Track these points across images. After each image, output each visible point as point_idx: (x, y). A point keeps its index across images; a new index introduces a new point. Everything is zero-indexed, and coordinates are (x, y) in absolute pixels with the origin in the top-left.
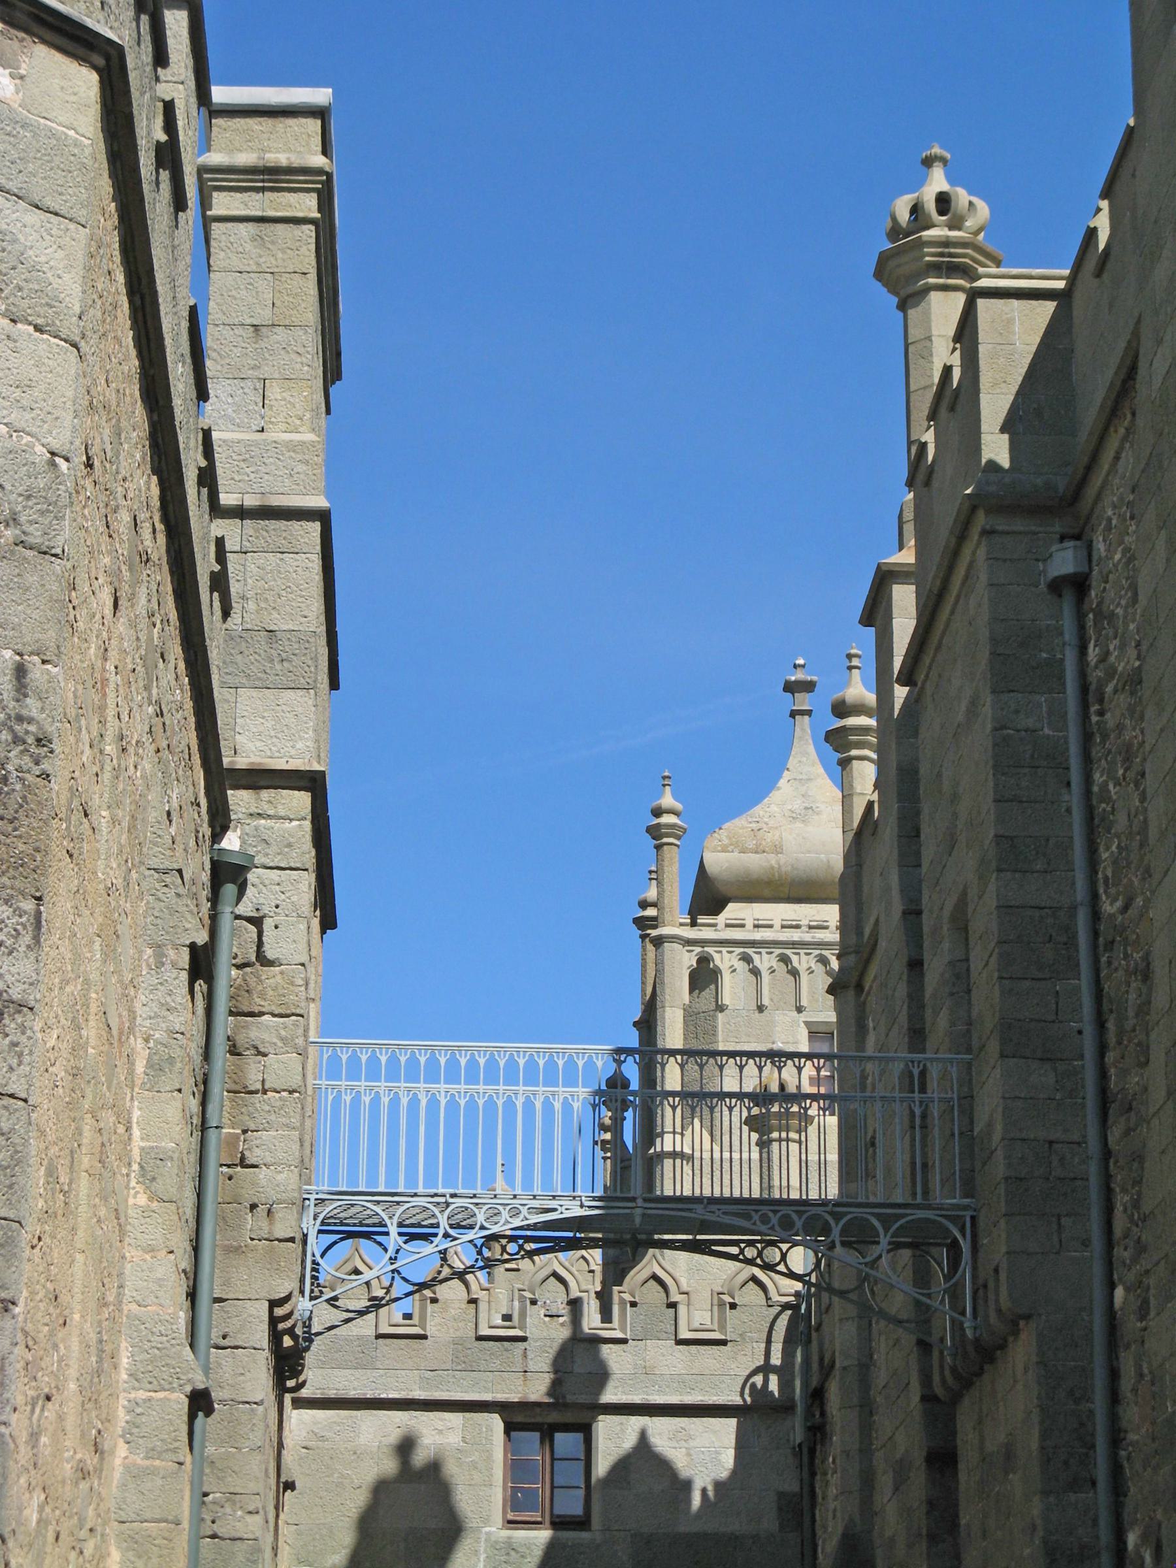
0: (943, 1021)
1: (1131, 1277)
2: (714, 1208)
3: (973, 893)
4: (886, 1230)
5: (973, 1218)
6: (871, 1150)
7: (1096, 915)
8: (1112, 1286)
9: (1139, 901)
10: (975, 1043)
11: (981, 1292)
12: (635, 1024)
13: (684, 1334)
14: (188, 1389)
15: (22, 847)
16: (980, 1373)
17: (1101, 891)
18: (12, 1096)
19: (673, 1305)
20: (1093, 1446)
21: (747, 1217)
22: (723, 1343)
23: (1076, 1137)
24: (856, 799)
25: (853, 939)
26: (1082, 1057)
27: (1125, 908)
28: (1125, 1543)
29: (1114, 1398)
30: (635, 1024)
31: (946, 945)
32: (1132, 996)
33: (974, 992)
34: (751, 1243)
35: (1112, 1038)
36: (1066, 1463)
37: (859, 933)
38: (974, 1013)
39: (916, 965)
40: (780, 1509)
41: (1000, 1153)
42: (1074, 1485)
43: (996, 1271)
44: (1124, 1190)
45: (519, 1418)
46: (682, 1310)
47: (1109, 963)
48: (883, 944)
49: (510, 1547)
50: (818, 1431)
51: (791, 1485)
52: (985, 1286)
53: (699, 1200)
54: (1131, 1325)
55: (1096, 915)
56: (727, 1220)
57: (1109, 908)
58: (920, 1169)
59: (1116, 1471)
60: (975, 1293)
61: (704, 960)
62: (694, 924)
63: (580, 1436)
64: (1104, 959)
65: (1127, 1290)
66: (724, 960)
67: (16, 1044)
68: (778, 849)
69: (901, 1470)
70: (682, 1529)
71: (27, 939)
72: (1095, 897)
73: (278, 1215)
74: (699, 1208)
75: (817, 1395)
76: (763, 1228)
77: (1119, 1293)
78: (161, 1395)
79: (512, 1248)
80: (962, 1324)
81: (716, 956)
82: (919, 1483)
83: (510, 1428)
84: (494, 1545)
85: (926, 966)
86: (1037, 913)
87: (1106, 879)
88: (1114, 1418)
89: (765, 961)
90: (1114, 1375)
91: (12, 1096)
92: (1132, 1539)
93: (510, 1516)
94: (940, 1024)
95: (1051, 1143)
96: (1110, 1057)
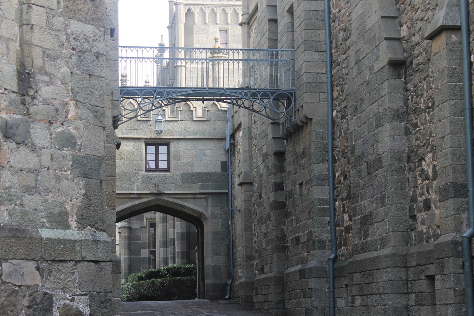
0: (284, 39)
1: (339, 109)
2: (226, 90)
3: (295, 6)
4: (272, 95)
5: (295, 93)
6: (252, 70)
7: (330, 13)
8: (333, 111)
9: (344, 10)
10: (296, 47)
11: (297, 112)
13: (195, 119)
14: (116, 143)
15: (100, 14)
16: (294, 133)
17: (331, 6)
18: (102, 77)
20: (327, 152)
21: (236, 93)
23: (324, 72)
25: (246, 10)
26: (326, 51)
27: (339, 11)
28: (335, 176)
29: (333, 139)
30: (167, 28)
31: (286, 18)
32: (341, 35)
33: (295, 33)
34: (234, 99)
35: (334, 45)
36: (320, 155)
37: (248, 9)
38: (295, 38)
39: (273, 21)
40: (222, 166)
41: (304, 76)
42: (322, 162)
43: (302, 106)
44: (337, 86)
45: (149, 142)
46: (194, 112)
47: (333, 26)
48: (259, 14)
49: (148, 177)
50: (233, 146)
51: (224, 159)
52: (298, 110)
53: (223, 89)
54: (338, 120)
55: (330, 13)
56: (230, 93)
57: (333, 11)
58: (274, 78)
59: (333, 157)
60: (295, 112)
61: (189, 10)
63: (166, 147)
64: (332, 25)
65: (337, 112)
66: (196, 11)
67: (102, 64)
69: (265, 157)
70: (195, 171)
71: (102, 38)
72: (329, 8)
73: (114, 94)
74: (223, 91)
75: (233, 136)
76: (240, 96)
77: (335, 112)
78: (109, 145)
79: (171, 101)
80: (291, 120)
81: (193, 8)
82: (271, 160)
83: (147, 144)
84: (143, 177)
85: (278, 23)
86: (314, 12)
87: (333, 4)
88: (333, 144)
89: (208, 11)
90: (333, 133)
91: (102, 77)
92: (337, 174)
94: (283, 41)
95: (317, 73)
96: (333, 51)
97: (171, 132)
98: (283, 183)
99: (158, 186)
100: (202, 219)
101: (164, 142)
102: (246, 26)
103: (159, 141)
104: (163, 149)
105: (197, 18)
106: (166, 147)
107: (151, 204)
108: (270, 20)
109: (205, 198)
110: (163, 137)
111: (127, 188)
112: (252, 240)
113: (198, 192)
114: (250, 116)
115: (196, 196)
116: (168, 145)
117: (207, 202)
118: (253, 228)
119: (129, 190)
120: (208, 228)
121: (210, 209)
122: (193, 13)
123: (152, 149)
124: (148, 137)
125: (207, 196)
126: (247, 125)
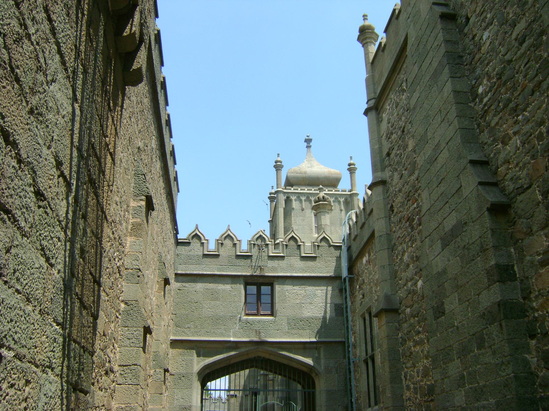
12: (269, 221)
19: (299, 246)
22: (314, 258)
24: (370, 54)
30: (269, 221)
40: (336, 310)
49: (247, 322)
51: (338, 301)
61: (288, 198)
62: (286, 189)
63: (270, 287)
66: (293, 198)
68: (305, 173)
83: (246, 284)
89: (303, 198)
93: (247, 312)
97: (274, 269)
98: (513, 266)
99: (260, 333)
100: (313, 375)
101: (266, 281)
102: (373, 114)
103: (261, 280)
104: (265, 289)
105: (295, 204)
106: (270, 287)
107: (252, 356)
108: (443, 16)
109: (316, 348)
110: (266, 274)
111: (222, 335)
112: (402, 396)
113: (308, 340)
114: (388, 218)
115: (307, 345)
116: (272, 285)
117: (319, 353)
118: (403, 377)
119: (224, 336)
120: (321, 386)
121: (322, 361)
122: (291, 200)
123: (253, 289)
124: (249, 274)
125: (318, 346)
126: (385, 230)
